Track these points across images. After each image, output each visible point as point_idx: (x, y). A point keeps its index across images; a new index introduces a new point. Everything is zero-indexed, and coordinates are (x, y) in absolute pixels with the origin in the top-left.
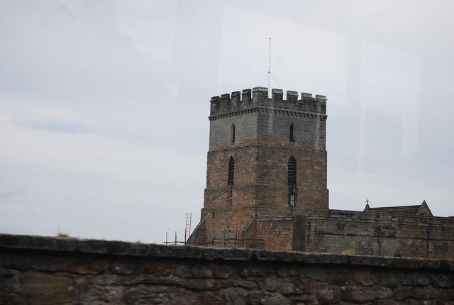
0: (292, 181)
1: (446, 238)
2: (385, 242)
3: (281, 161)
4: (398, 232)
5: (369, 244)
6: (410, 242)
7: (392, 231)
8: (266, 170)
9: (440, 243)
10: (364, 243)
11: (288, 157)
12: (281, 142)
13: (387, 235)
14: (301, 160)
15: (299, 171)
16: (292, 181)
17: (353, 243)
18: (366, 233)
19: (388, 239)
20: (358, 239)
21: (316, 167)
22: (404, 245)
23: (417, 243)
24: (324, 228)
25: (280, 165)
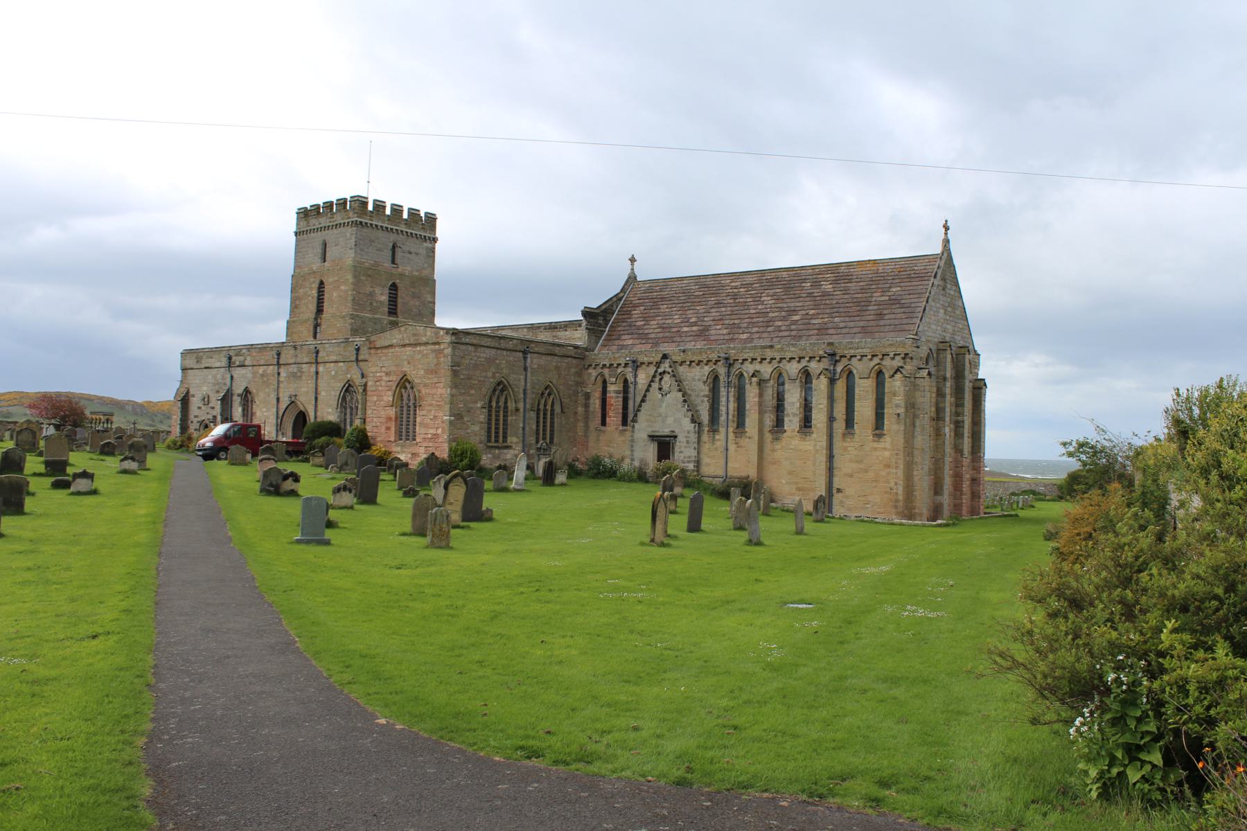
0: (320, 310)
1: (299, 360)
2: (238, 372)
3: (311, 289)
4: (249, 358)
5: (224, 378)
6: (261, 370)
7: (242, 358)
8: (297, 302)
9: (293, 369)
10: (219, 376)
11: (318, 282)
12: (313, 265)
13: (237, 363)
14: (328, 281)
15: (326, 296)
16: (320, 310)
17: (210, 377)
18: (218, 364)
19: (239, 368)
20: (214, 371)
21: (343, 288)
22: (254, 373)
23: (269, 372)
24: (191, 362)
25: (309, 293)
